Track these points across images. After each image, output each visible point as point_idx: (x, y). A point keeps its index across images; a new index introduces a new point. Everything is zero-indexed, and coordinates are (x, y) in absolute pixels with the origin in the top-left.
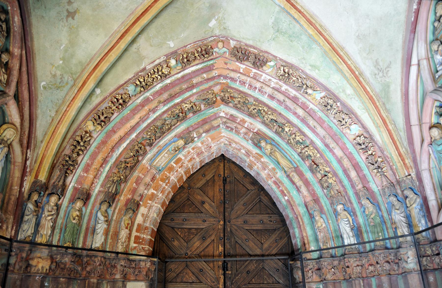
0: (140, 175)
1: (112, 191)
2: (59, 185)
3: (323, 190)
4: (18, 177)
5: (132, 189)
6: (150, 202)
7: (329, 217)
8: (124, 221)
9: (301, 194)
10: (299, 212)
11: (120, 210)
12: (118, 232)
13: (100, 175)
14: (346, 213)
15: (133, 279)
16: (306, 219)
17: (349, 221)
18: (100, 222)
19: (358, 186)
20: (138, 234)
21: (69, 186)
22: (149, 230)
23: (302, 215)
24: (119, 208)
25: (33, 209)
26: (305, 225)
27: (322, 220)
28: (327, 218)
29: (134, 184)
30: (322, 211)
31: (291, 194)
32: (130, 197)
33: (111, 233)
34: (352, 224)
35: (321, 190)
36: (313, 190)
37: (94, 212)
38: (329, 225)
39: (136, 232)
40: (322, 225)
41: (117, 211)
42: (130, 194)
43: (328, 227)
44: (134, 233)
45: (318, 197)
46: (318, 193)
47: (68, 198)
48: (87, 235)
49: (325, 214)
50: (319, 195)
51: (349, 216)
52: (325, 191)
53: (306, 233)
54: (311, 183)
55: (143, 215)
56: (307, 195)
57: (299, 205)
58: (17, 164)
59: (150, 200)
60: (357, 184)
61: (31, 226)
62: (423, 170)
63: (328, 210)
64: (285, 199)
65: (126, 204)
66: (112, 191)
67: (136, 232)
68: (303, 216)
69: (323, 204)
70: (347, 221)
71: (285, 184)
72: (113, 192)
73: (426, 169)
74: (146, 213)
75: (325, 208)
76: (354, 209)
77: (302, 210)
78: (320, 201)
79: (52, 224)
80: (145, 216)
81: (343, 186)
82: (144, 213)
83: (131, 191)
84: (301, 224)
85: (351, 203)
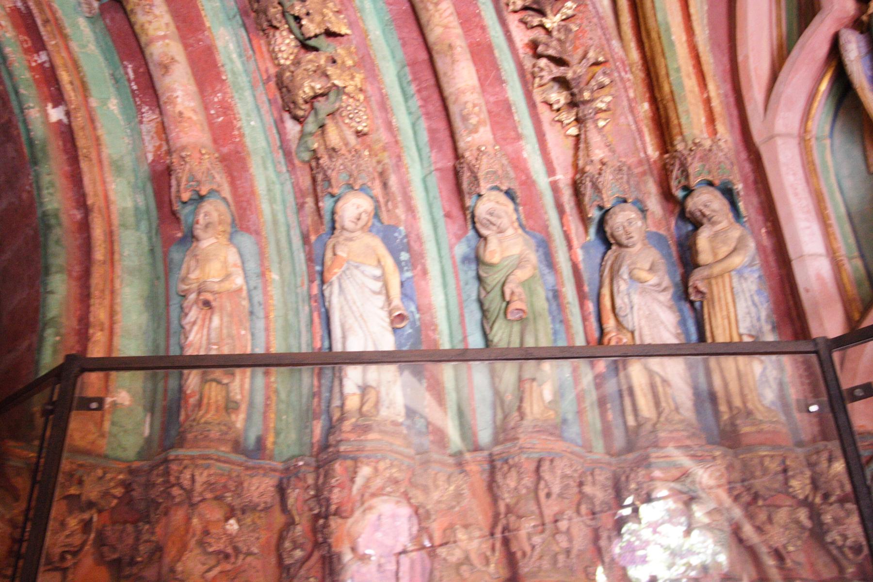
3: (279, 124)
7: (271, 251)
9: (150, 115)
10: (106, 197)
14: (377, 243)
16: (132, 246)
17: (384, 279)
19: (475, 130)
23: (116, 221)
26: (118, 270)
27: (232, 256)
28: (262, 255)
30: (243, 219)
31: (93, 102)
34: (397, 301)
35: (270, 120)
36: (226, 109)
38: (265, 292)
40: (228, 276)
43: (258, 297)
45: (242, 144)
46: (247, 131)
49: (257, 233)
50: (248, 140)
51: (389, 262)
52: (292, 128)
53: (112, 313)
54: (227, 76)
56: (188, 114)
57: (118, 169)
60: (474, 120)
62: (779, 135)
63: (275, 222)
64: (46, 115)
68: (124, 226)
69: (261, 187)
70: (377, 278)
71: (74, 45)
73: (788, 135)
75: (265, 207)
76: (419, 238)
77: (122, 195)
78: (245, 168)
81: (390, 127)
84: (99, 254)
85: (411, 209)
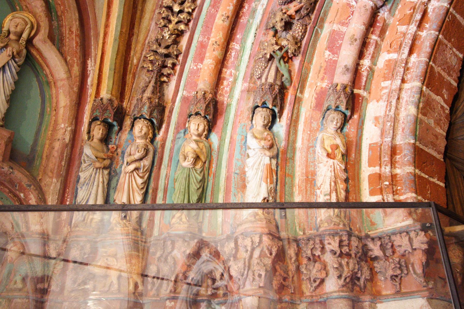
0: (336, 27)
1: (266, 79)
2: (145, 98)
4: (64, 107)
5: (324, 65)
6: (387, 83)
8: (323, 142)
11: (309, 122)
12: (314, 174)
13: (237, 58)
15: (389, 292)
18: (251, 152)
20: (376, 169)
21: (174, 101)
22: (406, 152)
24: (306, 119)
25: (94, 157)
29: (327, 53)
32: (324, 85)
33: (297, 181)
37: (238, 138)
39: (370, 165)
41: (301, 127)
42: (323, 79)
44: (366, 171)
47: (174, 123)
48: (230, 191)
55: (376, 119)
58: (59, 84)
59: (385, 78)
61: (94, 192)
65: (319, 104)
66: (266, 79)
67: (370, 165)
72: (271, 80)
74: (382, 114)
79: (140, 181)
80: (381, 120)
82: (378, 115)
83: (322, 71)
